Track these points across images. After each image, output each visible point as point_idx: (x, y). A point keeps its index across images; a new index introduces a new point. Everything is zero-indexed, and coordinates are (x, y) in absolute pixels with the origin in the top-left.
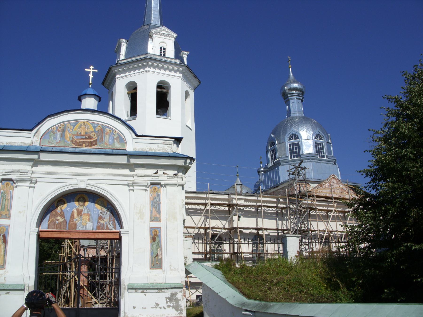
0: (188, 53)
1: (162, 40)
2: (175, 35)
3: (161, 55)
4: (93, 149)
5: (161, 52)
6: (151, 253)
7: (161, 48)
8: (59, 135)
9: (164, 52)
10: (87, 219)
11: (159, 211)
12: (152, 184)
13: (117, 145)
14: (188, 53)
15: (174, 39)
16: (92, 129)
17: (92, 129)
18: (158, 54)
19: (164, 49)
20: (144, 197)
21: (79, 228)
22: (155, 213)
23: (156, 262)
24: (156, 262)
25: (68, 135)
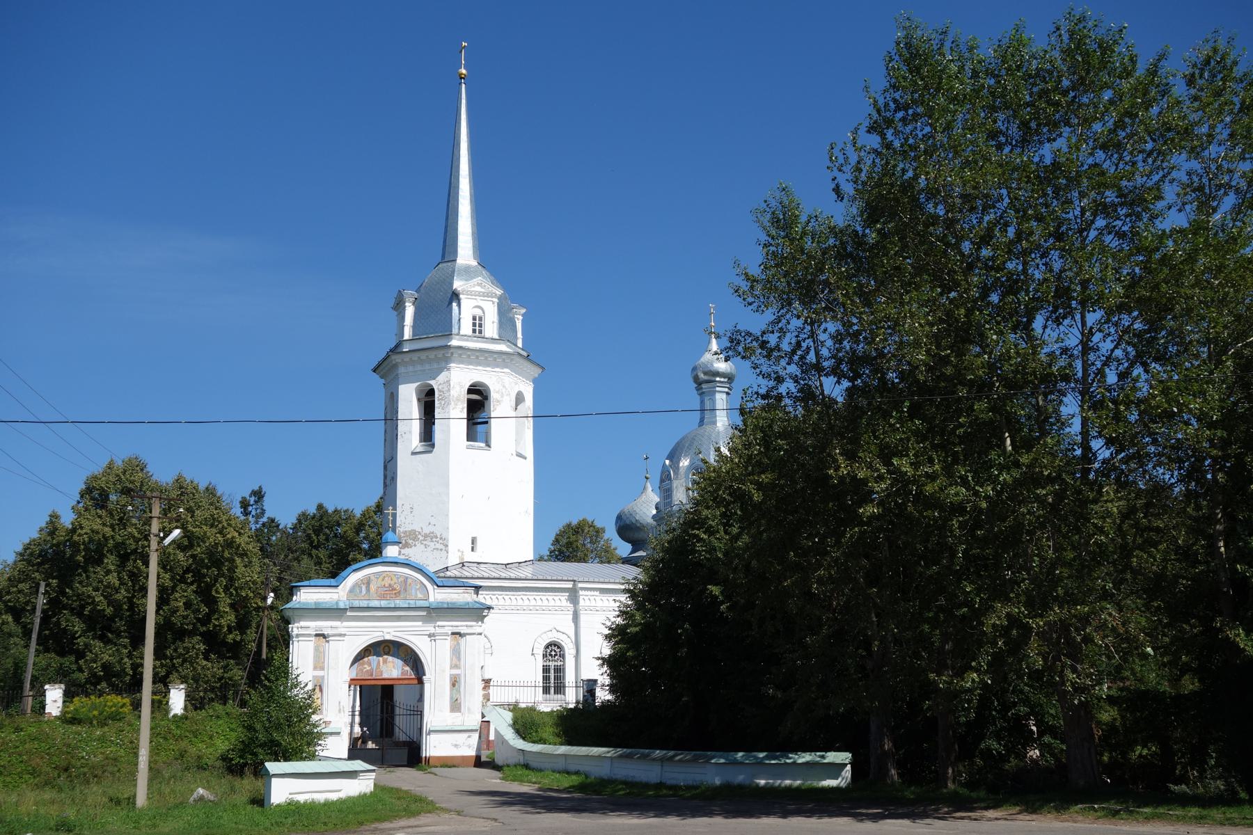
0: (524, 311)
1: (475, 303)
2: (499, 292)
3: (474, 331)
4: (400, 603)
5: (474, 325)
6: (451, 698)
7: (474, 318)
8: (364, 588)
9: (480, 325)
10: (392, 669)
11: (459, 659)
12: (453, 634)
13: (420, 596)
14: (524, 311)
15: (496, 300)
16: (395, 580)
17: (395, 580)
18: (470, 333)
19: (480, 319)
20: (445, 645)
21: (385, 676)
22: (455, 661)
23: (456, 706)
24: (456, 706)
25: (373, 587)
